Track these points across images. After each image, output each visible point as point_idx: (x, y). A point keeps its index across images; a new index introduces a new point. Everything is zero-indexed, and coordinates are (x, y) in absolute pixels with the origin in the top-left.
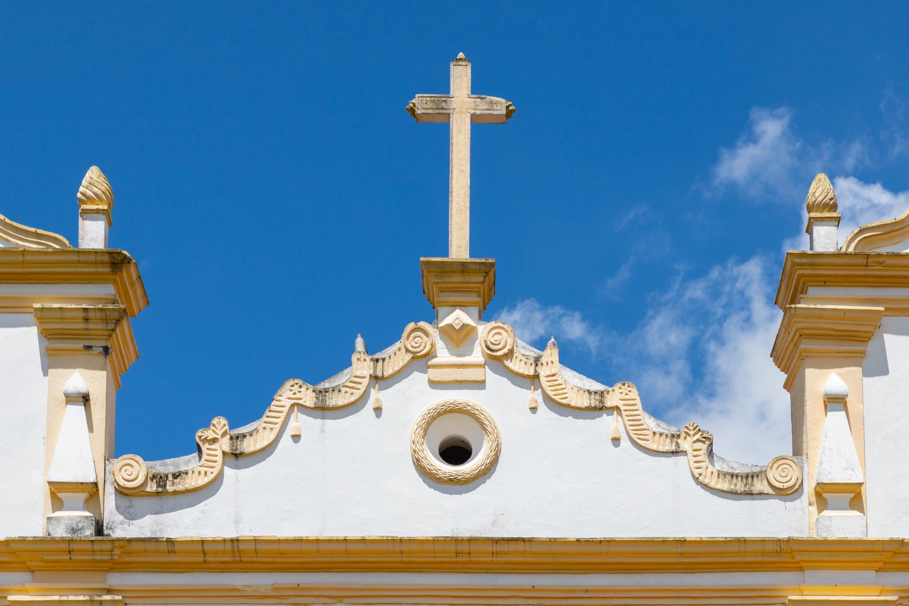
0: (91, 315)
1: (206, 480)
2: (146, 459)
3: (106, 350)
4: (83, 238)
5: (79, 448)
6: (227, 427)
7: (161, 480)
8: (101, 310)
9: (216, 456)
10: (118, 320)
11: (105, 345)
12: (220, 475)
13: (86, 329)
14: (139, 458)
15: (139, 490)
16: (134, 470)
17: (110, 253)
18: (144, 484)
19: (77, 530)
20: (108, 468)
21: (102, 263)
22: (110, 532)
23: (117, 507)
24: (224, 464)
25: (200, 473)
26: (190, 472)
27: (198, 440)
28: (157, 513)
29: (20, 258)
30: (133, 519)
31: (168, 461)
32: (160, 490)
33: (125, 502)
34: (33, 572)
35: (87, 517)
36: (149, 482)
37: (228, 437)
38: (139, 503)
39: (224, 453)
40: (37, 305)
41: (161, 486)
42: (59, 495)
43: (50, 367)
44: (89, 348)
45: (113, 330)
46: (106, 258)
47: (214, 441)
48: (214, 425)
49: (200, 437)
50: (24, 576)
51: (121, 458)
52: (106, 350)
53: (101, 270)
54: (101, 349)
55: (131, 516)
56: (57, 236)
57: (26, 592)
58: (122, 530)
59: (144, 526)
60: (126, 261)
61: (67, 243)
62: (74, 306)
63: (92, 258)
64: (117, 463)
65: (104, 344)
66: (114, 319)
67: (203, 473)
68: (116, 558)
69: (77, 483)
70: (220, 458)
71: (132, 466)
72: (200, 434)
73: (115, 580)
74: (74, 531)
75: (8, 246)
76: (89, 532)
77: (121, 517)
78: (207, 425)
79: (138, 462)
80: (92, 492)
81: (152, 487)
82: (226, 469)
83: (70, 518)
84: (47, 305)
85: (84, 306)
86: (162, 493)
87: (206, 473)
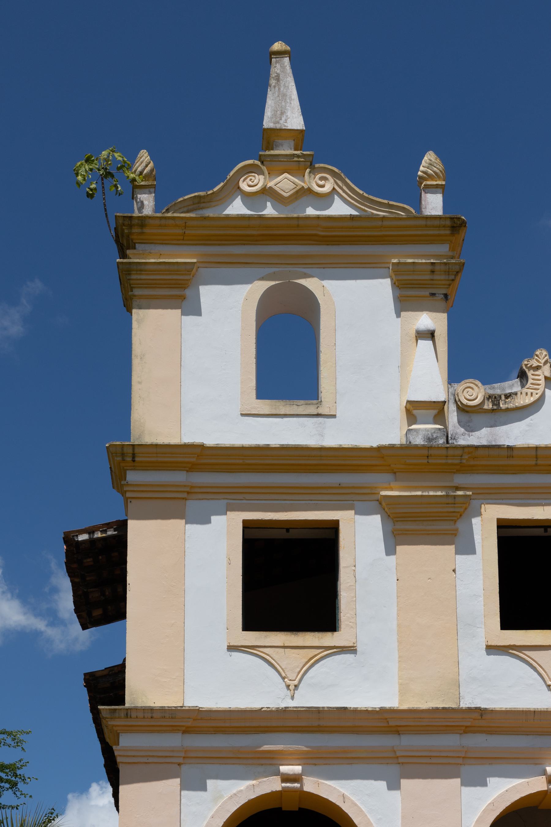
0: (437, 268)
1: (532, 399)
2: (484, 384)
3: (446, 296)
4: (426, 208)
5: (427, 375)
6: (547, 357)
7: (494, 399)
8: (445, 264)
9: (540, 380)
10: (457, 272)
11: (445, 292)
12: (543, 396)
13: (432, 280)
14: (478, 382)
15: (478, 408)
16: (474, 393)
17: (452, 219)
18: (483, 403)
19: (433, 439)
20: (450, 390)
21: (444, 226)
22: (454, 442)
23: (459, 422)
24: (546, 387)
25: (527, 394)
26: (519, 393)
27: (524, 367)
28: (491, 427)
29: (380, 223)
30: (472, 431)
31: (496, 385)
32: (495, 407)
33: (465, 417)
34: (395, 473)
35: (440, 429)
36: (486, 401)
37: (549, 365)
38: (477, 419)
39: (546, 378)
40: (395, 261)
41: (496, 405)
42: (415, 412)
43: (402, 311)
44: (433, 295)
45: (453, 280)
46: (448, 223)
47: (538, 368)
48: (537, 356)
49: (526, 365)
50: (388, 477)
51: (463, 382)
52: (446, 296)
53: (442, 232)
54: (442, 296)
55: (471, 429)
56: (405, 206)
57: (392, 489)
58: (464, 440)
59: (482, 437)
60: (463, 224)
61: (413, 211)
62: (424, 261)
63: (437, 223)
64: (459, 387)
65: (444, 291)
66: (454, 272)
67: (529, 394)
68: (464, 461)
69: (431, 402)
70: (542, 382)
71: (472, 388)
72: (526, 363)
73: (460, 479)
74: (429, 440)
75: (364, 214)
76: (441, 441)
77: (463, 430)
78: (531, 356)
79: (477, 386)
80: (437, 410)
81: (488, 406)
82: (547, 391)
83: (426, 430)
84: (402, 260)
85: (432, 261)
86: (497, 411)
87: (532, 393)
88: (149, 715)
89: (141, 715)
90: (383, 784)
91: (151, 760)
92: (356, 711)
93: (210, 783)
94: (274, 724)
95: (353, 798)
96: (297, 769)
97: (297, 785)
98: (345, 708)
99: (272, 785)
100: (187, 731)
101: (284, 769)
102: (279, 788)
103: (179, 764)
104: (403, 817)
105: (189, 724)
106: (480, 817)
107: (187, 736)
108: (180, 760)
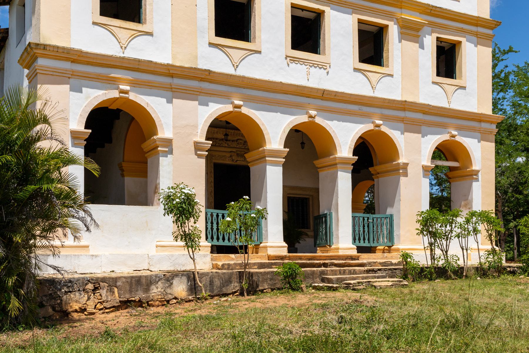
88: (56, 50)
89: (52, 49)
90: (164, 100)
91: (55, 74)
92: (156, 63)
93: (84, 89)
94: (117, 64)
95: (151, 105)
96: (128, 88)
97: (127, 95)
98: (152, 61)
99: (115, 94)
100: (73, 61)
101: (121, 87)
102: (118, 96)
103: (69, 78)
104: (173, 117)
105: (75, 58)
106: (206, 120)
107: (73, 64)
108: (70, 76)
